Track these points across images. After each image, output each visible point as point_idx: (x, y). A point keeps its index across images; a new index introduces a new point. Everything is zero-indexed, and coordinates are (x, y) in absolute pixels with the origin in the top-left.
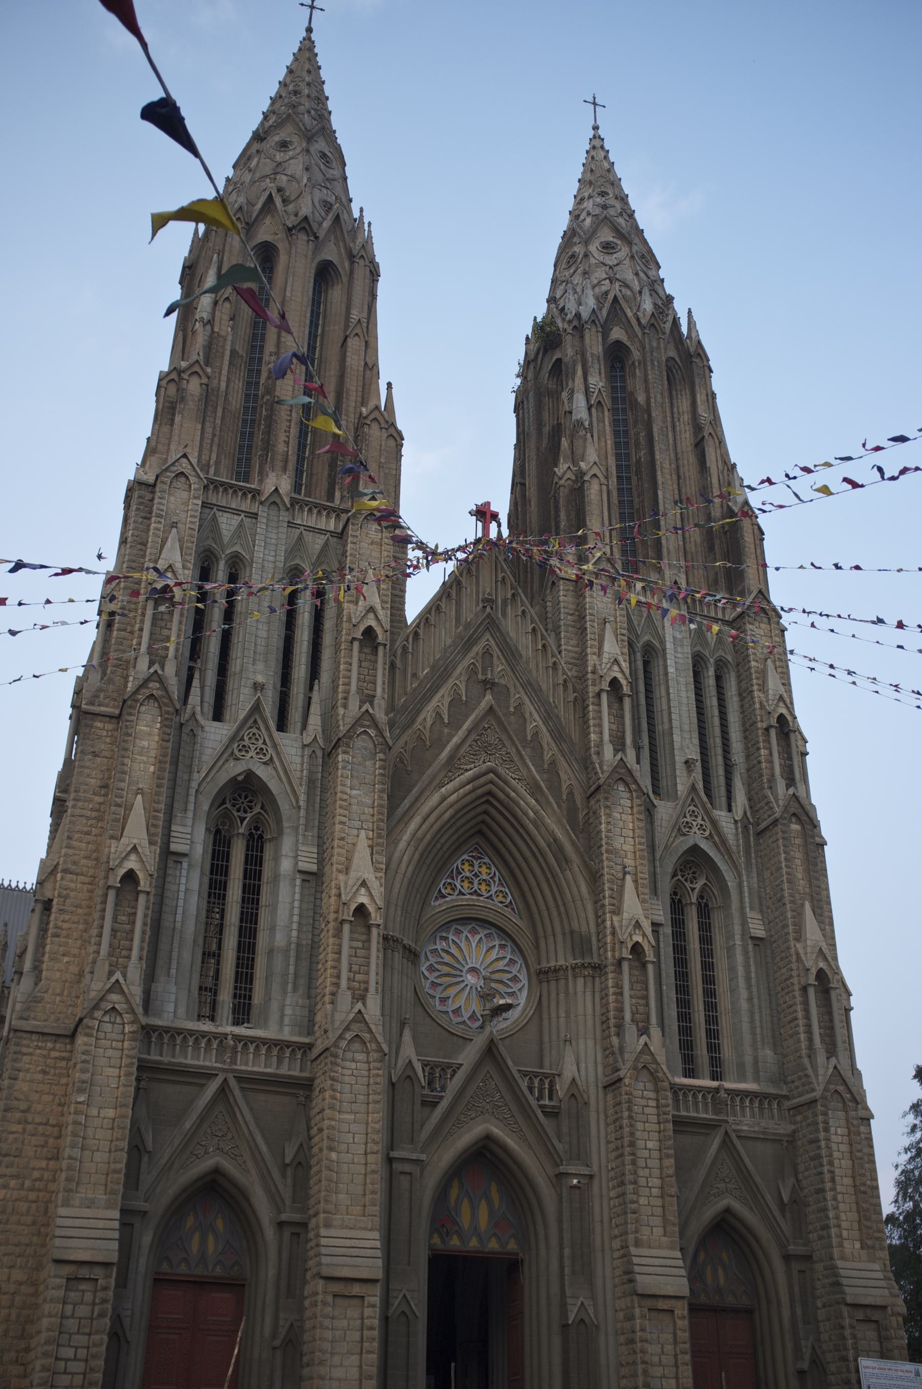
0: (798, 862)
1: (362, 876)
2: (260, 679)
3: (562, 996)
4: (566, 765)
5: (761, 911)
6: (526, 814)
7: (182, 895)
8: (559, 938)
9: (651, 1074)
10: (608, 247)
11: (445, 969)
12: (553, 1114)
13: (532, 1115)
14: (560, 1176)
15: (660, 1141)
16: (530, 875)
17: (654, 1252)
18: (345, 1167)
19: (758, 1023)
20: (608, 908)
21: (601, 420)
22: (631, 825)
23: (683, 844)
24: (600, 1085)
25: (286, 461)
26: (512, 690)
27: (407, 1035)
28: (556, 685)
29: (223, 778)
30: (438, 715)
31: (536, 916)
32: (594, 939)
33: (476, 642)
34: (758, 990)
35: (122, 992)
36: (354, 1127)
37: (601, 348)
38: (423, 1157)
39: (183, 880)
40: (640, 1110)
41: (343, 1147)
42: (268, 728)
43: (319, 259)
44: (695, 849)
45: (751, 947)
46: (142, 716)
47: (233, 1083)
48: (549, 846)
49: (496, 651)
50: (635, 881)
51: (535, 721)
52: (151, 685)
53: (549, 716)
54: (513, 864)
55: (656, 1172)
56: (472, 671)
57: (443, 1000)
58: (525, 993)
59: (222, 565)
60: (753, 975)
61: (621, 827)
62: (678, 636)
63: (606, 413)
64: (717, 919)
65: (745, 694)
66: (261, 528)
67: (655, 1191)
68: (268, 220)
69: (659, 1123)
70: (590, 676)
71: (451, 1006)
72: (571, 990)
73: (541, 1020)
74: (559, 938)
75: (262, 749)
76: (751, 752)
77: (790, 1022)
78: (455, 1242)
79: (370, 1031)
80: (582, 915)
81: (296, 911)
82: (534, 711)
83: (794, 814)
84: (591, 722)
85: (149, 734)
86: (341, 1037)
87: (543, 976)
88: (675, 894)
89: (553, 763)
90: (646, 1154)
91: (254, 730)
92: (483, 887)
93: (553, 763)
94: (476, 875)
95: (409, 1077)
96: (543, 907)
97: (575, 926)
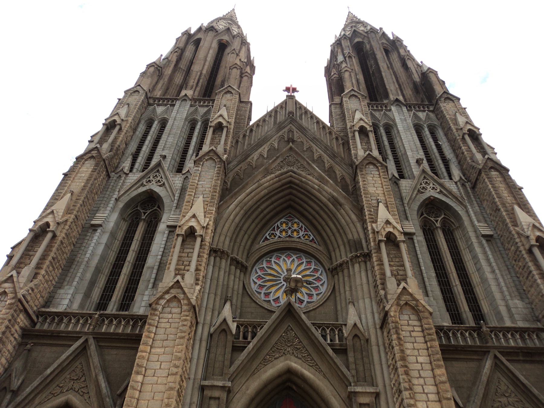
0: (503, 189)
2: (164, 154)
3: (346, 279)
4: (339, 168)
5: (486, 221)
6: (314, 188)
7: (93, 245)
8: (342, 247)
9: (413, 308)
11: (268, 278)
12: (342, 351)
13: (323, 351)
14: (352, 396)
15: (429, 356)
16: (320, 220)
18: (148, 388)
19: (503, 284)
20: (368, 221)
22: (380, 182)
24: (378, 327)
26: (305, 143)
27: (228, 306)
28: (331, 140)
29: (135, 193)
31: (328, 241)
32: (364, 241)
33: (284, 127)
34: (497, 264)
35: (13, 282)
36: (162, 358)
37: (349, 43)
38: (229, 384)
39: (96, 238)
40: (408, 334)
41: (149, 372)
42: (164, 172)
43: (219, 38)
45: (484, 242)
46: (85, 165)
47: (91, 341)
48: (329, 200)
49: (295, 130)
50: (387, 207)
51: (318, 151)
52: (93, 152)
53: (326, 149)
54: (311, 217)
55: (431, 381)
56: (282, 137)
57: (267, 295)
58: (325, 286)
59: (156, 122)
60: (491, 256)
61: (373, 184)
63: (353, 58)
64: (458, 234)
65: (448, 132)
67: (432, 397)
69: (426, 342)
70: (349, 130)
71: (271, 298)
72: (351, 273)
73: (335, 297)
74: (342, 247)
75: (159, 181)
76: (455, 149)
77: (527, 278)
79: (184, 293)
80: (354, 230)
81: (163, 246)
82: (318, 149)
83: (492, 168)
84: (351, 147)
85: (87, 171)
86: (161, 298)
87: (334, 271)
88: (426, 226)
89: (331, 168)
90: (418, 366)
91: (157, 174)
92: (295, 233)
93: (331, 168)
94: (290, 228)
95: (224, 330)
96: (330, 234)
97: (350, 236)
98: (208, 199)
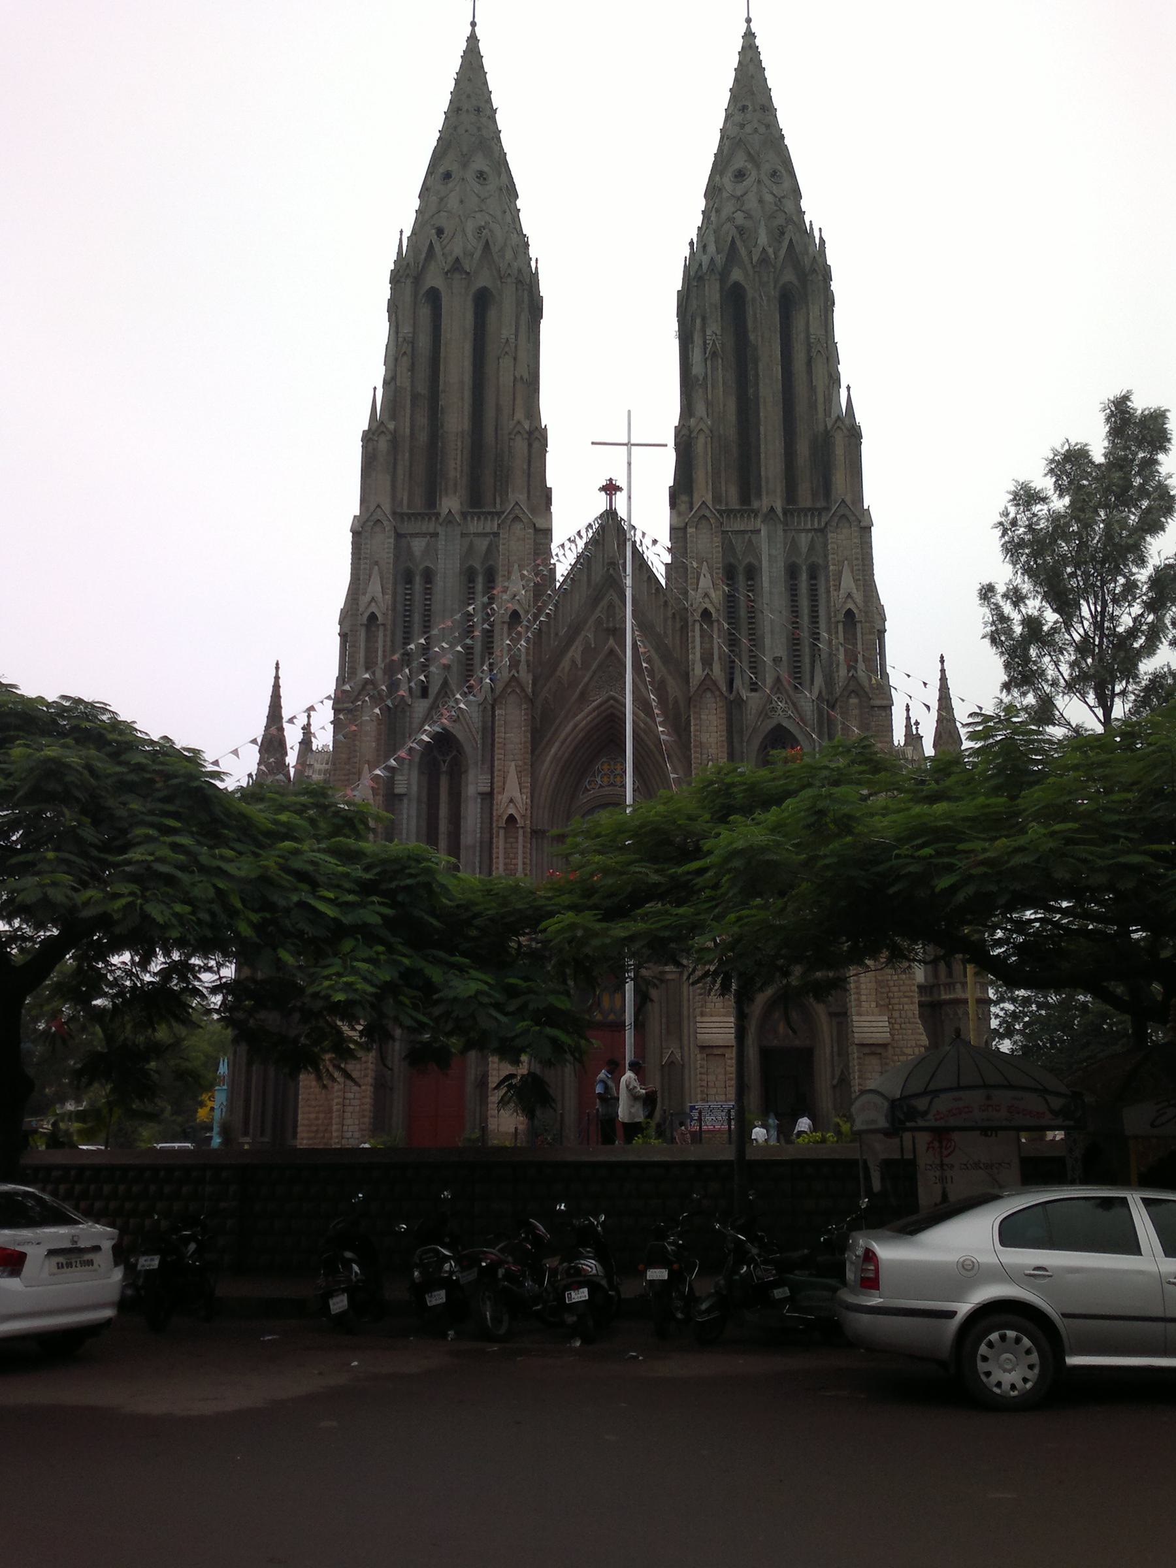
1: (514, 795)
7: (405, 821)
10: (740, 175)
17: (714, 1019)
21: (714, 369)
23: (769, 725)
25: (455, 485)
28: (665, 620)
30: (573, 661)
39: (405, 811)
43: (473, 290)
44: (779, 727)
56: (599, 621)
59: (418, 579)
62: (774, 552)
66: (441, 544)
68: (433, 267)
78: (598, 1017)
81: (479, 821)
98: (520, 763)
